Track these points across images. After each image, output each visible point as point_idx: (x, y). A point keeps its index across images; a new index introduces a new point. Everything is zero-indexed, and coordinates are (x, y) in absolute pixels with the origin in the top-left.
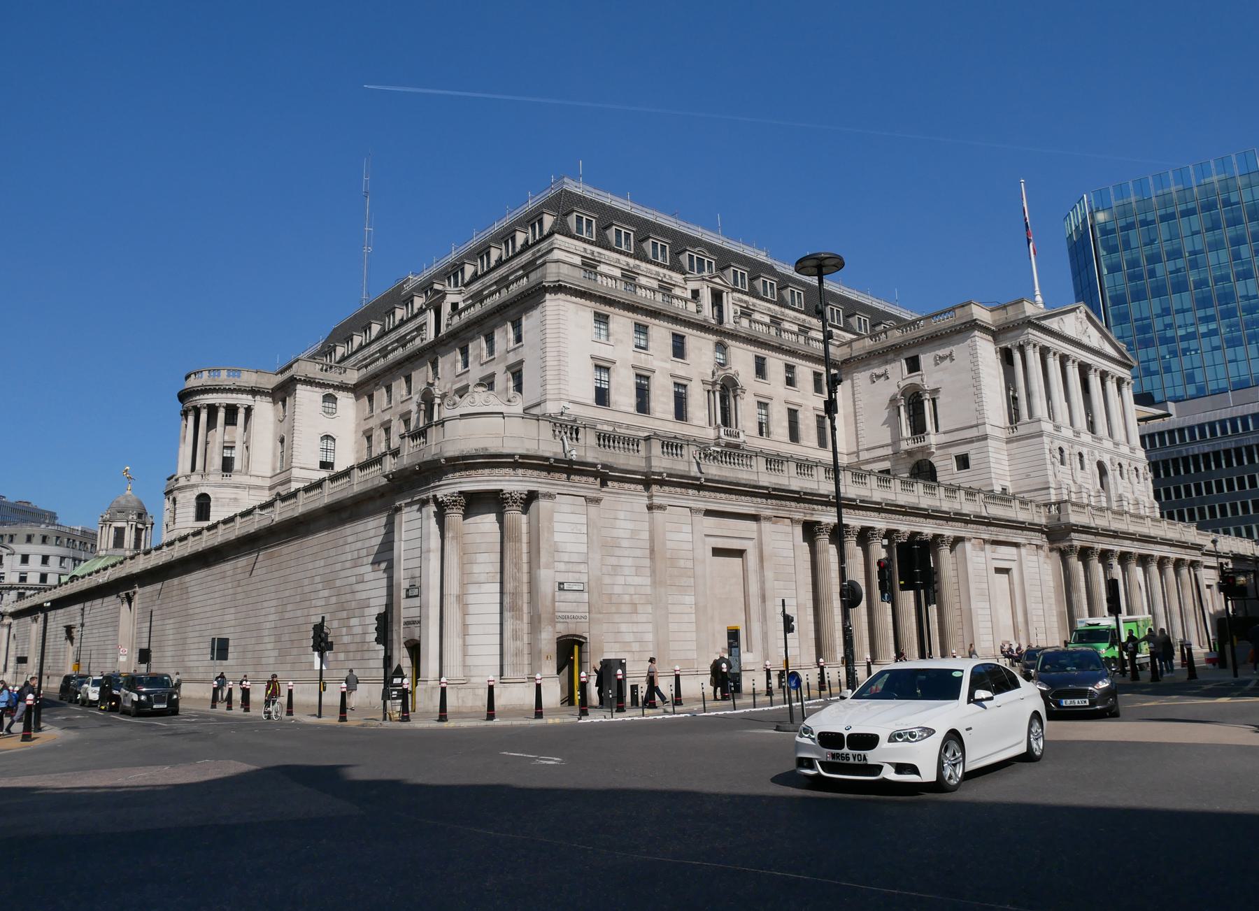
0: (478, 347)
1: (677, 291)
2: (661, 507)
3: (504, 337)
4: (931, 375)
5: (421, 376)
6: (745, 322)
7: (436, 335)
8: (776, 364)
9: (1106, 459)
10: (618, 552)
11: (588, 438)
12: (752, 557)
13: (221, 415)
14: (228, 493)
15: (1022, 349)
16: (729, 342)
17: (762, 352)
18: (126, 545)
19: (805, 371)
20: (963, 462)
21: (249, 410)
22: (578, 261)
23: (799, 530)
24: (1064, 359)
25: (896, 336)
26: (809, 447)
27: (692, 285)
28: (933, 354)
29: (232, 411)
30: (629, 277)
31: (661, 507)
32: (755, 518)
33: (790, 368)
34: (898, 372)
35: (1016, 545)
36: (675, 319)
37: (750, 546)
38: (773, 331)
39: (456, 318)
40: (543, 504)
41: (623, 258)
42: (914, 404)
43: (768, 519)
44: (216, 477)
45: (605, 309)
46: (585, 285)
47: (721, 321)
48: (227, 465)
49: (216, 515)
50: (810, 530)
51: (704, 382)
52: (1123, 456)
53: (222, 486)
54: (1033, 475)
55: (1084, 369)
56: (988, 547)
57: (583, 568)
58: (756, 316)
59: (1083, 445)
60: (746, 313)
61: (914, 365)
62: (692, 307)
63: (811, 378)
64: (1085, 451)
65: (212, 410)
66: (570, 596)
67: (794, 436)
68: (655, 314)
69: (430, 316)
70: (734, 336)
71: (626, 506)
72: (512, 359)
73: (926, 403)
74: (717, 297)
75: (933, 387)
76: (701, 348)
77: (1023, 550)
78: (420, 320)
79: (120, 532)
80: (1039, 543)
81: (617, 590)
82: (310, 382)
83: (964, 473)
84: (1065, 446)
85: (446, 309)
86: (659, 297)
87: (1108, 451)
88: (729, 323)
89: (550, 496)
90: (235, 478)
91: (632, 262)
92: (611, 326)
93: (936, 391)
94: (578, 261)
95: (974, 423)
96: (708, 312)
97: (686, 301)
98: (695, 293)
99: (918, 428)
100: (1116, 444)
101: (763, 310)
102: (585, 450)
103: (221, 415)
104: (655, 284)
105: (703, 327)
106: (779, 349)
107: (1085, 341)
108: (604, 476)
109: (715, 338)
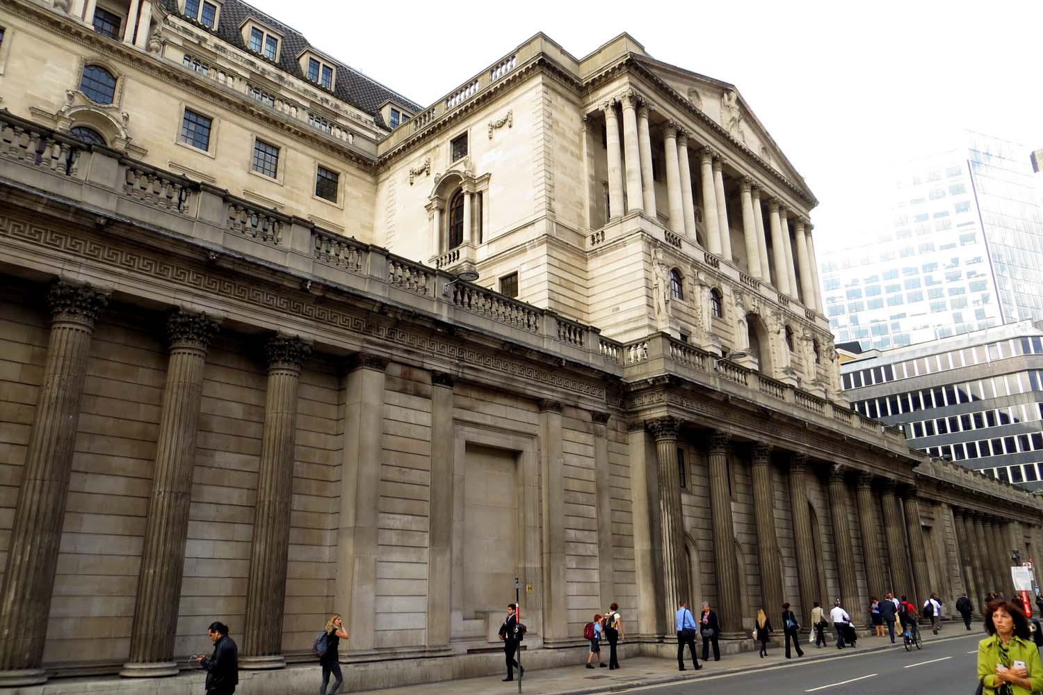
9: (766, 313)
15: (618, 107)
16: (118, 66)
24: (696, 155)
28: (487, 121)
34: (439, 158)
35: (540, 405)
42: (455, 202)
52: (794, 317)
54: (622, 307)
55: (734, 189)
56: (443, 391)
59: (726, 279)
61: (460, 145)
64: (726, 290)
70: (138, 61)
73: (467, 199)
75: (479, 173)
77: (555, 419)
80: (600, 408)
84: (687, 270)
93: (487, 178)
95: (528, 221)
99: (456, 238)
100: (784, 299)
109: (91, 54)
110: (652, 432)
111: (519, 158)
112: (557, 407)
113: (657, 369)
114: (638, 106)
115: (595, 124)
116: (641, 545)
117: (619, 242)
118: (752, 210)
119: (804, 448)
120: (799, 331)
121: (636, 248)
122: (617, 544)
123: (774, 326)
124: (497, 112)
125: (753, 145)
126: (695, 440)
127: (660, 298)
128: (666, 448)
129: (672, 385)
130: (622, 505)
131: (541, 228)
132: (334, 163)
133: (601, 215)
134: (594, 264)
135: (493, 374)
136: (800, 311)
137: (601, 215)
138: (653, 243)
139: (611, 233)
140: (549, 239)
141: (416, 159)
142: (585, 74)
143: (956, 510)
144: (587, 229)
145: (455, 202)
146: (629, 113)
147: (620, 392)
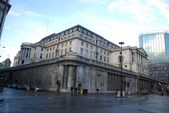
0: (65, 44)
1: (92, 40)
2: (92, 69)
3: (68, 44)
4: (123, 55)
5: (56, 47)
6: (100, 45)
7: (59, 42)
8: (103, 51)
9: (144, 68)
10: (86, 74)
11: (84, 59)
12: (101, 76)
13: (27, 49)
14: (27, 60)
15: (135, 52)
17: (102, 49)
18: (7, 65)
19: (107, 52)
20: (126, 66)
21: (31, 49)
22: (80, 35)
23: (107, 73)
24: (140, 54)
25: (119, 49)
26: (106, 62)
27: (94, 40)
29: (28, 49)
30: (86, 38)
31: (92, 69)
32: (102, 71)
33: (105, 52)
36: (91, 44)
37: (101, 75)
38: (103, 47)
39: (62, 40)
40: (78, 67)
41: (86, 35)
42: (121, 58)
43: (104, 71)
44: (25, 58)
45: (83, 41)
46: (81, 38)
47: (97, 45)
48: (27, 56)
49: (25, 63)
50: (109, 73)
51: (94, 52)
52: (145, 67)
53: (26, 59)
55: (142, 56)
57: (82, 76)
58: (101, 44)
59: (141, 65)
60: (100, 44)
61: (121, 53)
62: (94, 42)
63: (107, 53)
65: (26, 48)
66: (80, 79)
67: (105, 61)
68: (89, 43)
69: (58, 39)
70: (98, 47)
71: (87, 68)
72: (70, 47)
74: (97, 41)
76: (94, 48)
78: (56, 39)
79: (7, 64)
81: (85, 79)
82: (40, 46)
83: (126, 68)
85: (61, 39)
86: (90, 41)
87: (144, 67)
88: (98, 45)
89: (79, 66)
90: (28, 58)
91: (87, 36)
92: (83, 44)
94: (80, 35)
96: (95, 44)
97: (92, 41)
98: (94, 40)
100: (145, 66)
101: (102, 44)
102: (83, 61)
103: (27, 49)
104: (89, 39)
105: (95, 45)
106: (104, 49)
107: (142, 52)
108: (85, 64)
110: (138, 79)
111: (127, 56)
112: (133, 78)
113: (138, 75)
114: (136, 52)
115: (133, 53)
116: (137, 86)
117: (134, 64)
118: (143, 58)
119: (146, 79)
120: (146, 69)
121: (136, 65)
122: (135, 86)
123: (144, 69)
124: (125, 51)
125: (143, 52)
126: (140, 79)
127: (137, 69)
128: (139, 80)
129: (140, 76)
130: (136, 83)
131: (129, 62)
132: (109, 52)
133: (133, 61)
134: (132, 65)
135: (131, 76)
136: (146, 67)
137: (133, 61)
138: (137, 64)
139: (134, 63)
140: (130, 64)
141: (116, 53)
142: (132, 49)
143: (157, 83)
144: (132, 62)
145: (121, 58)
146: (136, 53)
147: (136, 76)
